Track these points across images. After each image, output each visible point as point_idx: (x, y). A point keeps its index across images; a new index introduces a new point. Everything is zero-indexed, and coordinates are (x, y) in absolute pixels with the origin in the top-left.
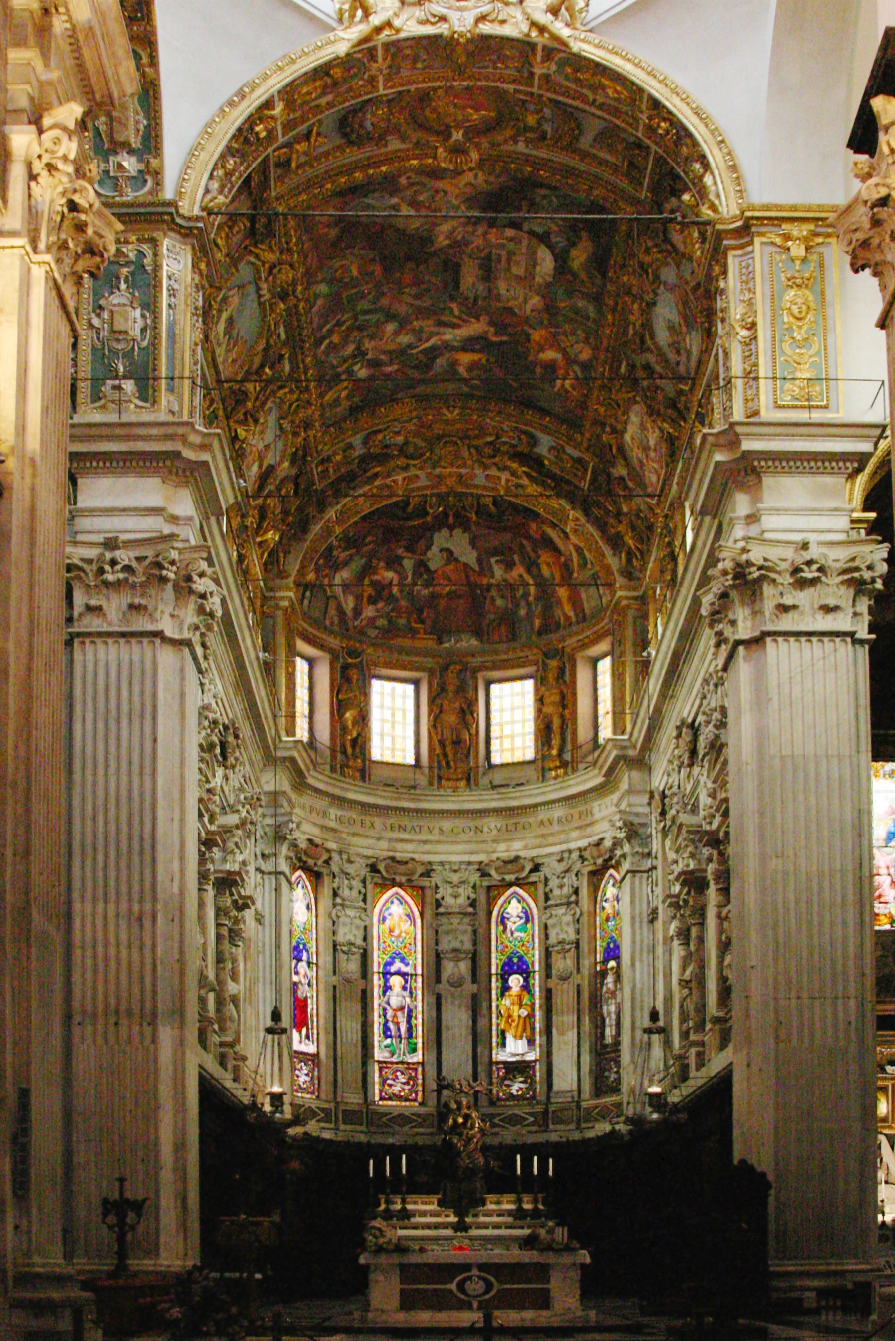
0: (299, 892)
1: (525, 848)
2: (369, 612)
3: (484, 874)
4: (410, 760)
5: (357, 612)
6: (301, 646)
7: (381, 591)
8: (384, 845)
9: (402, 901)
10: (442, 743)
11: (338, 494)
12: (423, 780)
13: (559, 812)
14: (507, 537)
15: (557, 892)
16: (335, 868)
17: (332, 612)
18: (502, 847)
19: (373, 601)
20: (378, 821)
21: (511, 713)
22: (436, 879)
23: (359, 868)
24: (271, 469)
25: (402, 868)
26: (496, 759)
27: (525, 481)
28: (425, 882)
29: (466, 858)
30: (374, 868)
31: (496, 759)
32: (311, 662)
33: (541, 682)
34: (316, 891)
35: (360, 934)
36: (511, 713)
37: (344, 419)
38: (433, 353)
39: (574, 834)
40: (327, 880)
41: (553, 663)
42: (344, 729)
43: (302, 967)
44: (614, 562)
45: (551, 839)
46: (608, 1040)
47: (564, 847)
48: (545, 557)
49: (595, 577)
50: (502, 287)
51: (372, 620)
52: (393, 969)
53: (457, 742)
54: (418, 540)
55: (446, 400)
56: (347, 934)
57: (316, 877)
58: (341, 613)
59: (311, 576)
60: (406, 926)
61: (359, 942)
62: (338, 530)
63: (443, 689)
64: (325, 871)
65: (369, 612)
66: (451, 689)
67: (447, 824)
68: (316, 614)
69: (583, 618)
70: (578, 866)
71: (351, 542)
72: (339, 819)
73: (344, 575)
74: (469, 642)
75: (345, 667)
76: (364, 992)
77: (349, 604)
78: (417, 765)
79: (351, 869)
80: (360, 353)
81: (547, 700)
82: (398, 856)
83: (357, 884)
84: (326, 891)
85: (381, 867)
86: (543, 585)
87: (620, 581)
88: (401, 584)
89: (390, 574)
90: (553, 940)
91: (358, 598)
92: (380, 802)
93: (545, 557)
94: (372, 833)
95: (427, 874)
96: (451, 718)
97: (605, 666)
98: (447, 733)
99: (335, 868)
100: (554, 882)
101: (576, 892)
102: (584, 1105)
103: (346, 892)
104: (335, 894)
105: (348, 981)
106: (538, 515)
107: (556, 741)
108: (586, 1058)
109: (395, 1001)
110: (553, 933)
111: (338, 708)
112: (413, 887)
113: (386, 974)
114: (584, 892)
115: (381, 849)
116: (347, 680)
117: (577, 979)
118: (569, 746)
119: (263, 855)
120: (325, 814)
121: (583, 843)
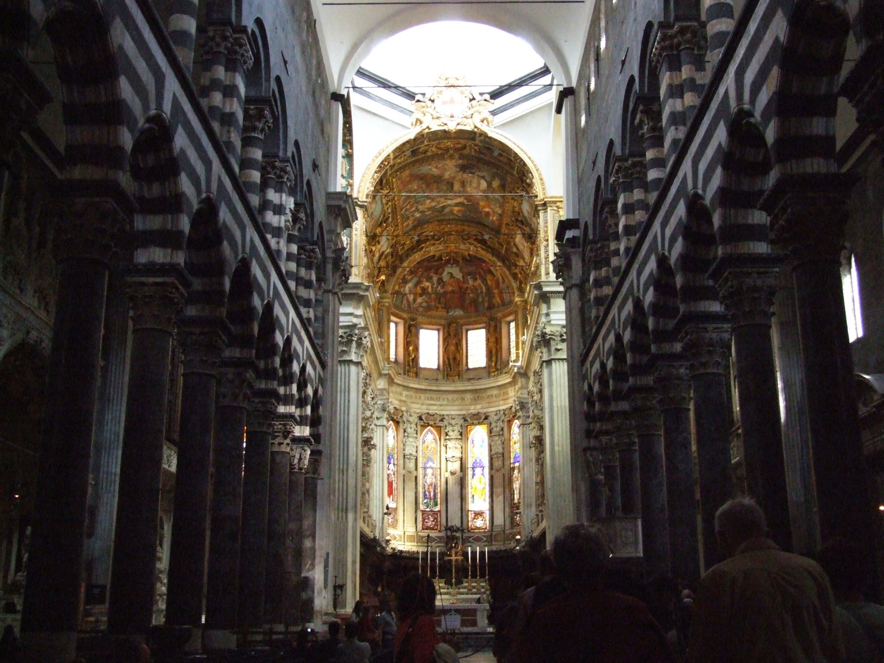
0: (390, 430)
1: (482, 408)
2: (419, 300)
3: (465, 420)
4: (436, 367)
5: (415, 300)
6: (393, 318)
7: (424, 291)
8: (425, 407)
9: (432, 433)
10: (448, 359)
11: (408, 256)
12: (440, 377)
13: (495, 392)
14: (472, 269)
15: (495, 429)
16: (405, 419)
17: (405, 302)
18: (472, 407)
19: (421, 295)
20: (422, 396)
21: (476, 344)
22: (445, 422)
23: (414, 419)
24: (383, 252)
25: (432, 418)
26: (471, 366)
27: (479, 249)
28: (441, 424)
29: (458, 413)
30: (420, 418)
31: (471, 366)
32: (396, 324)
33: (488, 332)
34: (397, 429)
35: (415, 450)
36: (476, 344)
37: (410, 230)
38: (444, 207)
39: (502, 403)
40: (401, 424)
41: (493, 323)
42: (409, 355)
43: (391, 466)
44: (515, 285)
45: (493, 404)
46: (516, 501)
47: (497, 408)
48: (489, 277)
49: (508, 287)
50: (469, 189)
51: (421, 303)
52: (428, 465)
53: (455, 358)
54: (438, 270)
55: (449, 221)
56: (409, 450)
57: (397, 423)
58: (408, 301)
59: (397, 288)
60: (433, 445)
61: (414, 453)
62: (408, 269)
63: (449, 335)
64: (401, 421)
65: (419, 300)
66: (452, 334)
67: (450, 397)
68: (398, 303)
69: (504, 304)
70: (503, 417)
71: (411, 272)
72: (406, 396)
73: (410, 285)
74: (459, 312)
75: (410, 326)
76: (416, 477)
77: (411, 297)
78: (438, 368)
79: (411, 419)
80: (417, 210)
81: (491, 340)
82: (431, 412)
83: (413, 426)
84: (402, 431)
85: (423, 418)
86: (489, 289)
87: (517, 293)
88: (432, 288)
89: (428, 284)
90: (493, 452)
91: (415, 294)
92: (423, 387)
93: (489, 277)
94: (419, 401)
95: (442, 420)
96: (452, 348)
97: (513, 325)
98: (451, 357)
99: (405, 419)
100: (493, 425)
101: (502, 429)
102: (507, 532)
103: (409, 430)
104: (405, 431)
105: (410, 472)
106: (484, 261)
107: (494, 359)
108: (507, 510)
109: (429, 481)
110: (493, 448)
111: (407, 344)
112: (437, 427)
113: (425, 468)
114: (506, 430)
115: (423, 409)
116: (410, 331)
117: (503, 470)
118: (499, 363)
119: (377, 418)
120: (401, 394)
121: (504, 407)
